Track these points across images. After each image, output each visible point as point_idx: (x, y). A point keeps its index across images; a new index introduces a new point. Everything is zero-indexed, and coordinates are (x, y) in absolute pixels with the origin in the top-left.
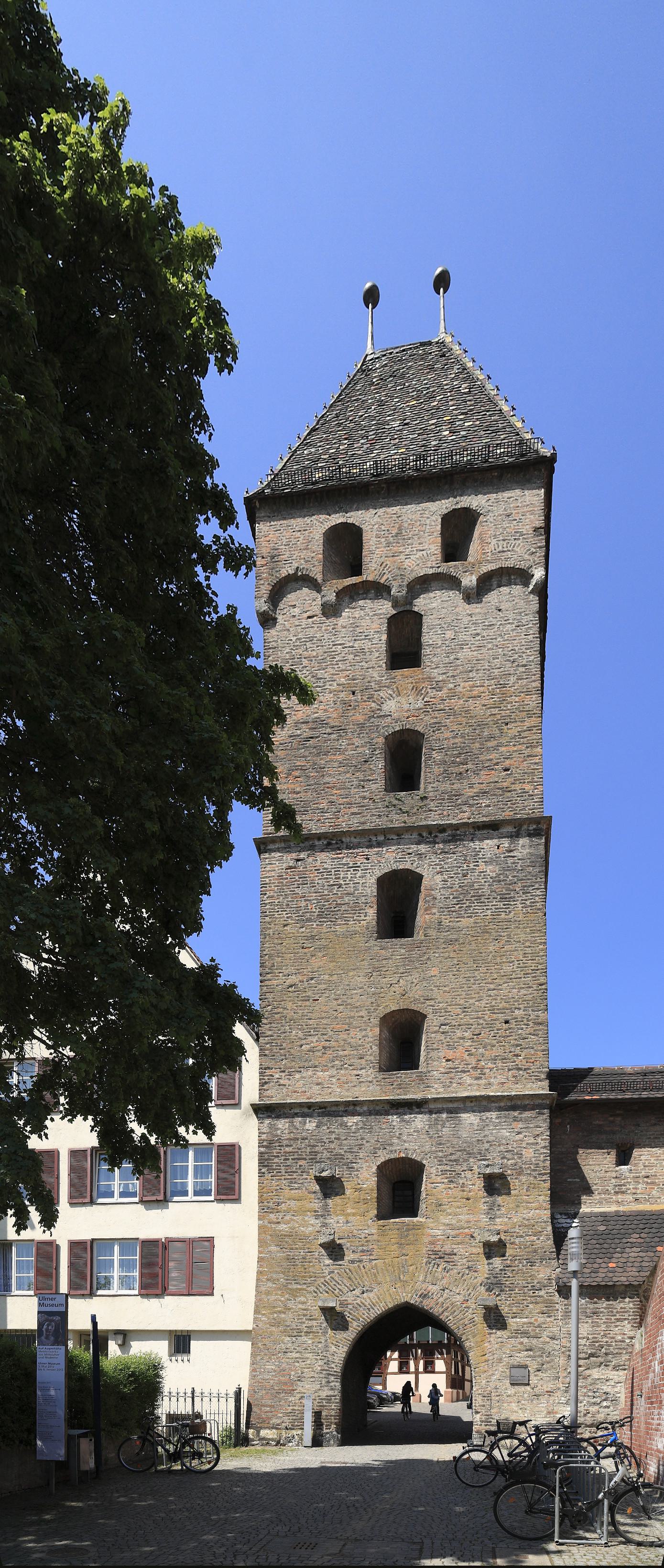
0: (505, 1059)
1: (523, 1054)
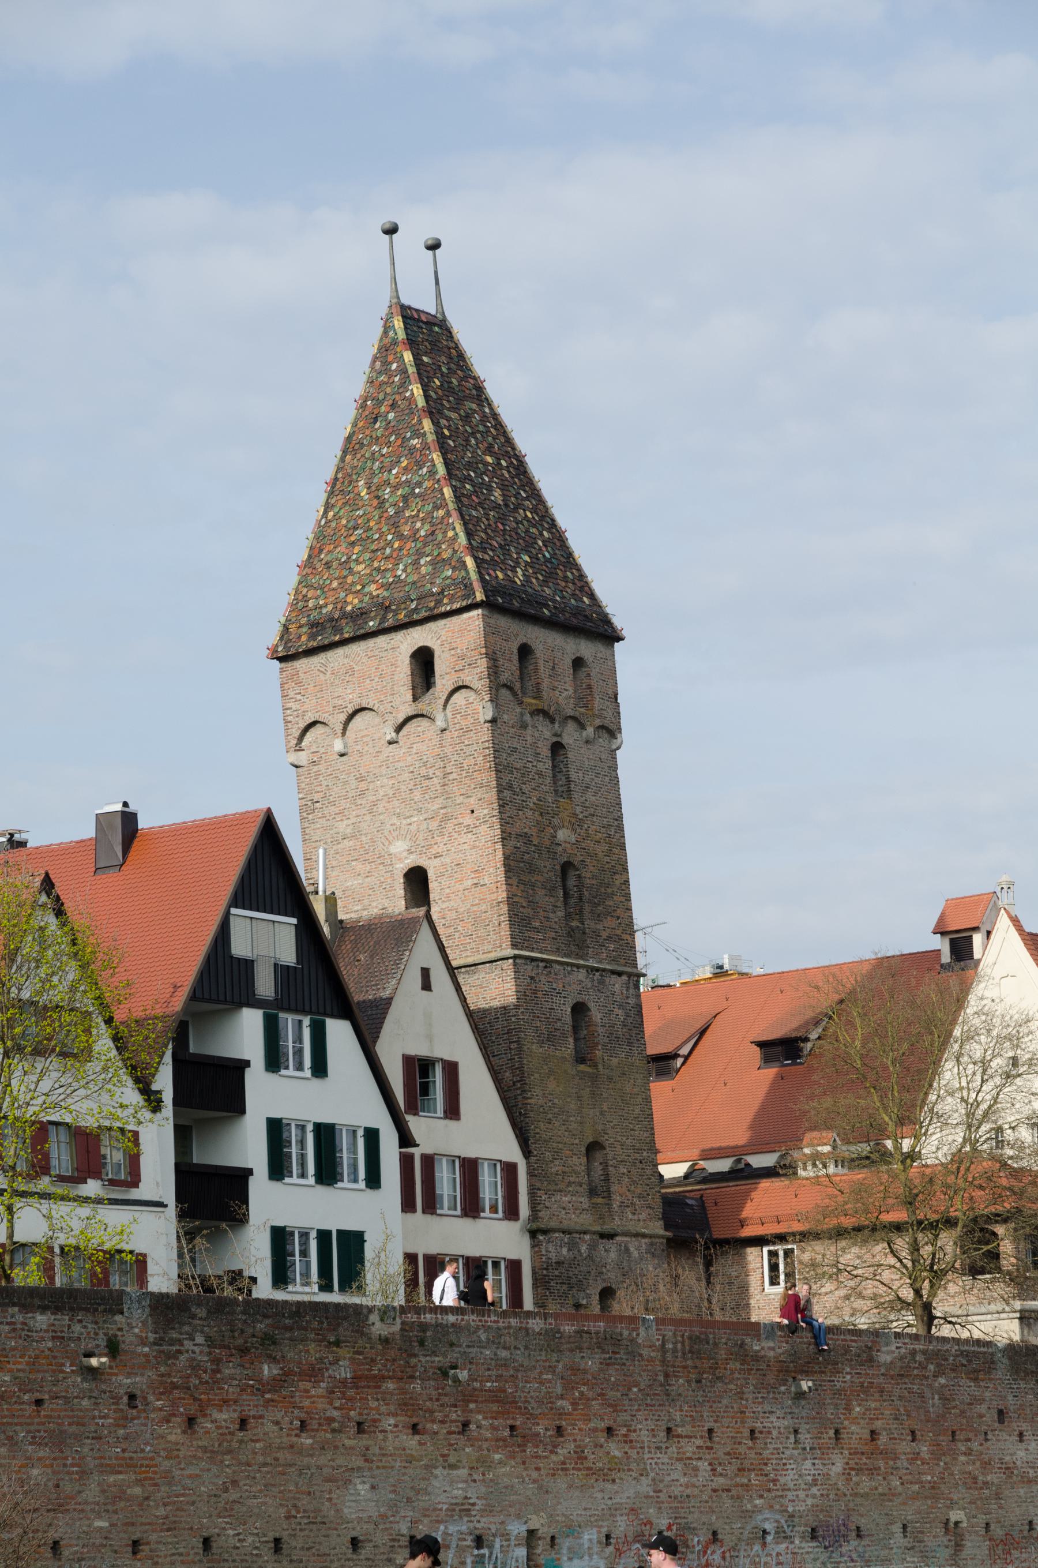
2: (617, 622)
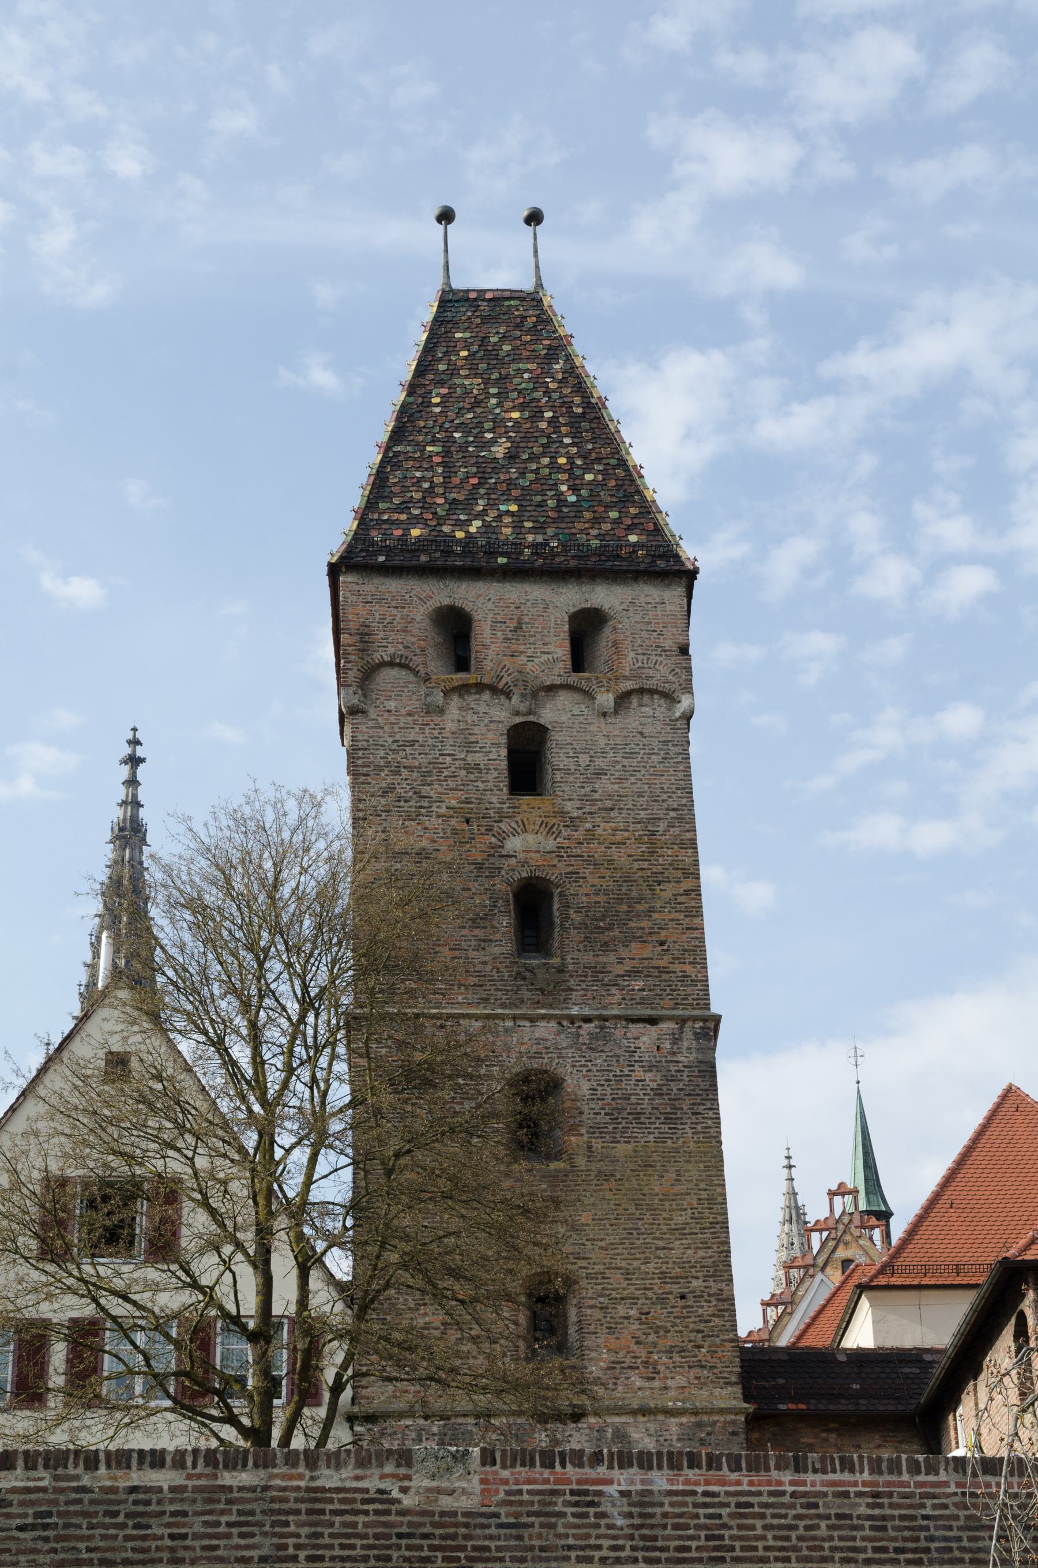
0: (684, 1351)
1: (706, 1344)
2: (689, 551)
